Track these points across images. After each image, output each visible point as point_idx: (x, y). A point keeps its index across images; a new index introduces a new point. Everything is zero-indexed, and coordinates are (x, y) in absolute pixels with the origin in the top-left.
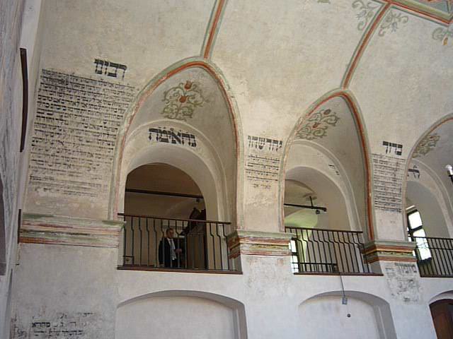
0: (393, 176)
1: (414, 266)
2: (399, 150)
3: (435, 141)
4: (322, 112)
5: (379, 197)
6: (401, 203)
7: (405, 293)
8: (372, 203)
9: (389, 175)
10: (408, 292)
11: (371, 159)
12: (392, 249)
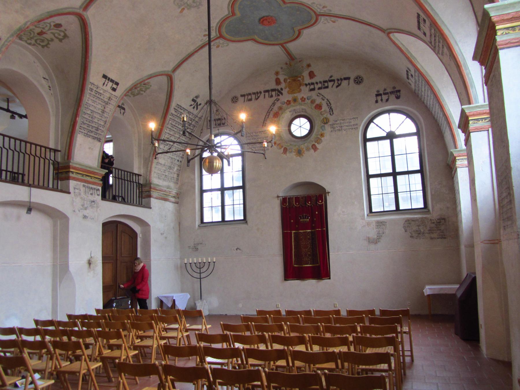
0: (103, 108)
1: (98, 190)
2: (115, 86)
3: (146, 89)
4: (52, 24)
5: (84, 124)
6: (103, 134)
7: (85, 211)
8: (77, 127)
9: (99, 106)
10: (88, 211)
11: (88, 86)
12: (83, 172)
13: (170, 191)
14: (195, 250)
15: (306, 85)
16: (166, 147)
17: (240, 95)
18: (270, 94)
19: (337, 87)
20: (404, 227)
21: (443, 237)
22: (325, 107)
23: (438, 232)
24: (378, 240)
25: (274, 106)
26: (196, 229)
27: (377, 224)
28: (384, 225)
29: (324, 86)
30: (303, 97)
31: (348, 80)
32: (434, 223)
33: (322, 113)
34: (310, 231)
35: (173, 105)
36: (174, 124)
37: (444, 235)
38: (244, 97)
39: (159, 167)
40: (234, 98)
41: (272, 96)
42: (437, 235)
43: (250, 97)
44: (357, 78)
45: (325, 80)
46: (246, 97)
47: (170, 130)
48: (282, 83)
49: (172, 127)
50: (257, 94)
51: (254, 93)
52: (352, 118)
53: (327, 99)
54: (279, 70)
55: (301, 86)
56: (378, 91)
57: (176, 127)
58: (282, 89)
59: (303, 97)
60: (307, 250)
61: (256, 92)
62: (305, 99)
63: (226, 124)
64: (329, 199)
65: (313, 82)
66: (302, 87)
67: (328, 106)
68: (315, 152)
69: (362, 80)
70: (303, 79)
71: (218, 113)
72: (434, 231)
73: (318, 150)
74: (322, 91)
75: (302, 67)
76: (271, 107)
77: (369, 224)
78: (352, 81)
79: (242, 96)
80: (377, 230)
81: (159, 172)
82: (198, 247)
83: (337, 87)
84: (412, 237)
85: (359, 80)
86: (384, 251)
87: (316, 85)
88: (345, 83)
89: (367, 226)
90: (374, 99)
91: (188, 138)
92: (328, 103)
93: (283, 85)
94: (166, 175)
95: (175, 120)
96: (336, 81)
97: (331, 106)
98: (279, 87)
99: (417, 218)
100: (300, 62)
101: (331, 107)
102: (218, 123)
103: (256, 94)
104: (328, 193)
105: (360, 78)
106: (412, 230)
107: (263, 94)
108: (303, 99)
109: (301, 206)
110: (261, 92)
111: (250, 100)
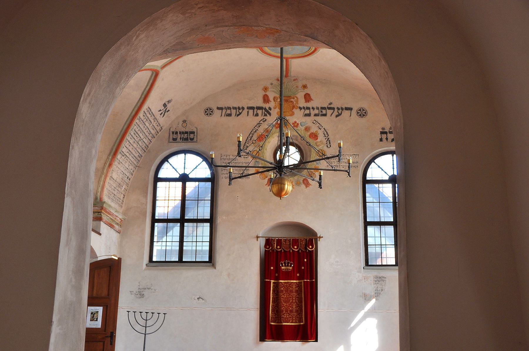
13: (116, 216)
14: (140, 296)
15: (300, 108)
16: (123, 158)
17: (216, 108)
18: (255, 113)
19: (337, 116)
22: (321, 137)
25: (259, 127)
26: (143, 269)
27: (376, 280)
29: (322, 113)
30: (295, 122)
31: (350, 111)
33: (318, 144)
35: (145, 108)
36: (137, 130)
38: (221, 111)
39: (111, 182)
40: (207, 110)
41: (257, 115)
43: (229, 112)
44: (360, 110)
45: (323, 106)
46: (224, 111)
47: (132, 137)
48: (271, 102)
49: (134, 134)
50: (239, 110)
51: (235, 108)
52: (352, 154)
53: (324, 129)
54: (270, 86)
55: (294, 109)
56: (383, 129)
57: (137, 135)
58: (270, 109)
59: (295, 122)
61: (237, 107)
62: (298, 124)
63: (195, 140)
64: (321, 245)
65: (308, 106)
66: (294, 110)
67: (325, 137)
68: (306, 188)
69: (365, 113)
70: (297, 101)
71: (185, 125)
73: (310, 186)
74: (319, 119)
75: (297, 87)
76: (256, 127)
78: (354, 112)
79: (218, 108)
80: (375, 285)
81: (110, 189)
82: (144, 293)
83: (337, 116)
85: (362, 113)
86: (382, 311)
87: (311, 110)
88: (346, 113)
89: (363, 281)
90: (379, 136)
91: (143, 150)
92: (325, 133)
93: (272, 104)
94: (115, 195)
95: (139, 126)
96: (336, 110)
97: (329, 137)
98: (267, 106)
100: (294, 80)
101: (328, 138)
102: (184, 138)
103: (238, 110)
104: (320, 237)
105: (363, 110)
107: (246, 110)
108: (296, 124)
109: (283, 251)
110: (243, 108)
111: (230, 115)
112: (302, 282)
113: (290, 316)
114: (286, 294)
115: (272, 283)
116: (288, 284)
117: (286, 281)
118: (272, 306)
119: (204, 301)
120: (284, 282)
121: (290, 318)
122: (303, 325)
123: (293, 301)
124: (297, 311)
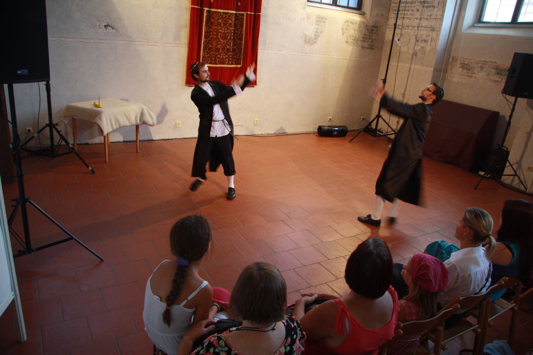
20: (343, 29)
21: (371, 48)
23: (370, 41)
24: (314, 40)
27: (318, 20)
28: (324, 22)
32: (368, 30)
34: (234, 12)
37: (373, 46)
42: (368, 45)
60: (225, 41)
72: (366, 39)
77: (309, 17)
80: (316, 27)
84: (347, 42)
89: (306, 19)
99: (355, 20)
106: (349, 35)
112: (243, 15)
113: (227, 56)
114: (225, 28)
115: (205, 11)
116: (227, 16)
117: (225, 11)
118: (204, 42)
119: (114, 31)
120: (222, 12)
121: (227, 58)
122: (240, 67)
123: (231, 37)
124: (234, 50)
